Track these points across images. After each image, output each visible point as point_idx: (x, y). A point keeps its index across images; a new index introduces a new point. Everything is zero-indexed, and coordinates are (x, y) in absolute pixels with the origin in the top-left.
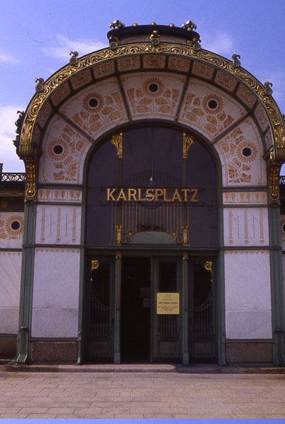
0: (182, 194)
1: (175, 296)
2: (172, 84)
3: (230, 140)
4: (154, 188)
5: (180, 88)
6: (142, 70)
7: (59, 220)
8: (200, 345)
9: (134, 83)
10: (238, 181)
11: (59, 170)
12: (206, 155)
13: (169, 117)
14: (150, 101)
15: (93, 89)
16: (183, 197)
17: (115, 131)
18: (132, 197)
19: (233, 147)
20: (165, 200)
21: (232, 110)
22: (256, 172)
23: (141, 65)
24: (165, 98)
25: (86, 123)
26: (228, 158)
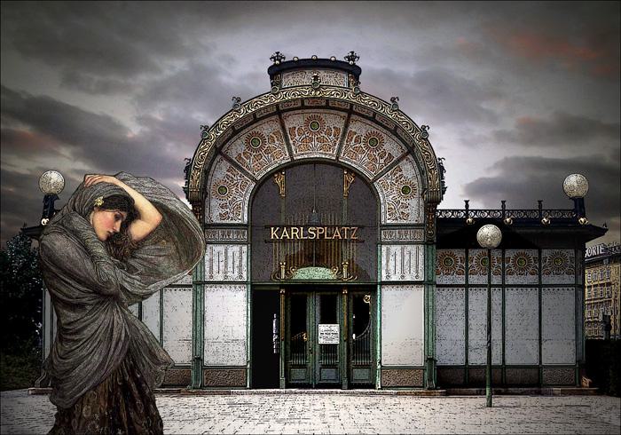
0: (342, 232)
1: (335, 328)
2: (334, 122)
3: (388, 179)
4: (315, 226)
5: (341, 126)
6: (303, 107)
7: (226, 258)
8: (353, 368)
9: (295, 121)
10: (396, 219)
11: (224, 211)
12: (366, 189)
13: (330, 155)
14: (311, 140)
15: (257, 128)
16: (343, 237)
17: (279, 170)
18: (295, 235)
19: (392, 184)
20: (326, 237)
21: (392, 147)
22: (413, 210)
23: (302, 105)
24: (326, 136)
25: (250, 162)
26: (388, 196)
